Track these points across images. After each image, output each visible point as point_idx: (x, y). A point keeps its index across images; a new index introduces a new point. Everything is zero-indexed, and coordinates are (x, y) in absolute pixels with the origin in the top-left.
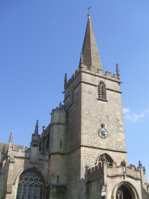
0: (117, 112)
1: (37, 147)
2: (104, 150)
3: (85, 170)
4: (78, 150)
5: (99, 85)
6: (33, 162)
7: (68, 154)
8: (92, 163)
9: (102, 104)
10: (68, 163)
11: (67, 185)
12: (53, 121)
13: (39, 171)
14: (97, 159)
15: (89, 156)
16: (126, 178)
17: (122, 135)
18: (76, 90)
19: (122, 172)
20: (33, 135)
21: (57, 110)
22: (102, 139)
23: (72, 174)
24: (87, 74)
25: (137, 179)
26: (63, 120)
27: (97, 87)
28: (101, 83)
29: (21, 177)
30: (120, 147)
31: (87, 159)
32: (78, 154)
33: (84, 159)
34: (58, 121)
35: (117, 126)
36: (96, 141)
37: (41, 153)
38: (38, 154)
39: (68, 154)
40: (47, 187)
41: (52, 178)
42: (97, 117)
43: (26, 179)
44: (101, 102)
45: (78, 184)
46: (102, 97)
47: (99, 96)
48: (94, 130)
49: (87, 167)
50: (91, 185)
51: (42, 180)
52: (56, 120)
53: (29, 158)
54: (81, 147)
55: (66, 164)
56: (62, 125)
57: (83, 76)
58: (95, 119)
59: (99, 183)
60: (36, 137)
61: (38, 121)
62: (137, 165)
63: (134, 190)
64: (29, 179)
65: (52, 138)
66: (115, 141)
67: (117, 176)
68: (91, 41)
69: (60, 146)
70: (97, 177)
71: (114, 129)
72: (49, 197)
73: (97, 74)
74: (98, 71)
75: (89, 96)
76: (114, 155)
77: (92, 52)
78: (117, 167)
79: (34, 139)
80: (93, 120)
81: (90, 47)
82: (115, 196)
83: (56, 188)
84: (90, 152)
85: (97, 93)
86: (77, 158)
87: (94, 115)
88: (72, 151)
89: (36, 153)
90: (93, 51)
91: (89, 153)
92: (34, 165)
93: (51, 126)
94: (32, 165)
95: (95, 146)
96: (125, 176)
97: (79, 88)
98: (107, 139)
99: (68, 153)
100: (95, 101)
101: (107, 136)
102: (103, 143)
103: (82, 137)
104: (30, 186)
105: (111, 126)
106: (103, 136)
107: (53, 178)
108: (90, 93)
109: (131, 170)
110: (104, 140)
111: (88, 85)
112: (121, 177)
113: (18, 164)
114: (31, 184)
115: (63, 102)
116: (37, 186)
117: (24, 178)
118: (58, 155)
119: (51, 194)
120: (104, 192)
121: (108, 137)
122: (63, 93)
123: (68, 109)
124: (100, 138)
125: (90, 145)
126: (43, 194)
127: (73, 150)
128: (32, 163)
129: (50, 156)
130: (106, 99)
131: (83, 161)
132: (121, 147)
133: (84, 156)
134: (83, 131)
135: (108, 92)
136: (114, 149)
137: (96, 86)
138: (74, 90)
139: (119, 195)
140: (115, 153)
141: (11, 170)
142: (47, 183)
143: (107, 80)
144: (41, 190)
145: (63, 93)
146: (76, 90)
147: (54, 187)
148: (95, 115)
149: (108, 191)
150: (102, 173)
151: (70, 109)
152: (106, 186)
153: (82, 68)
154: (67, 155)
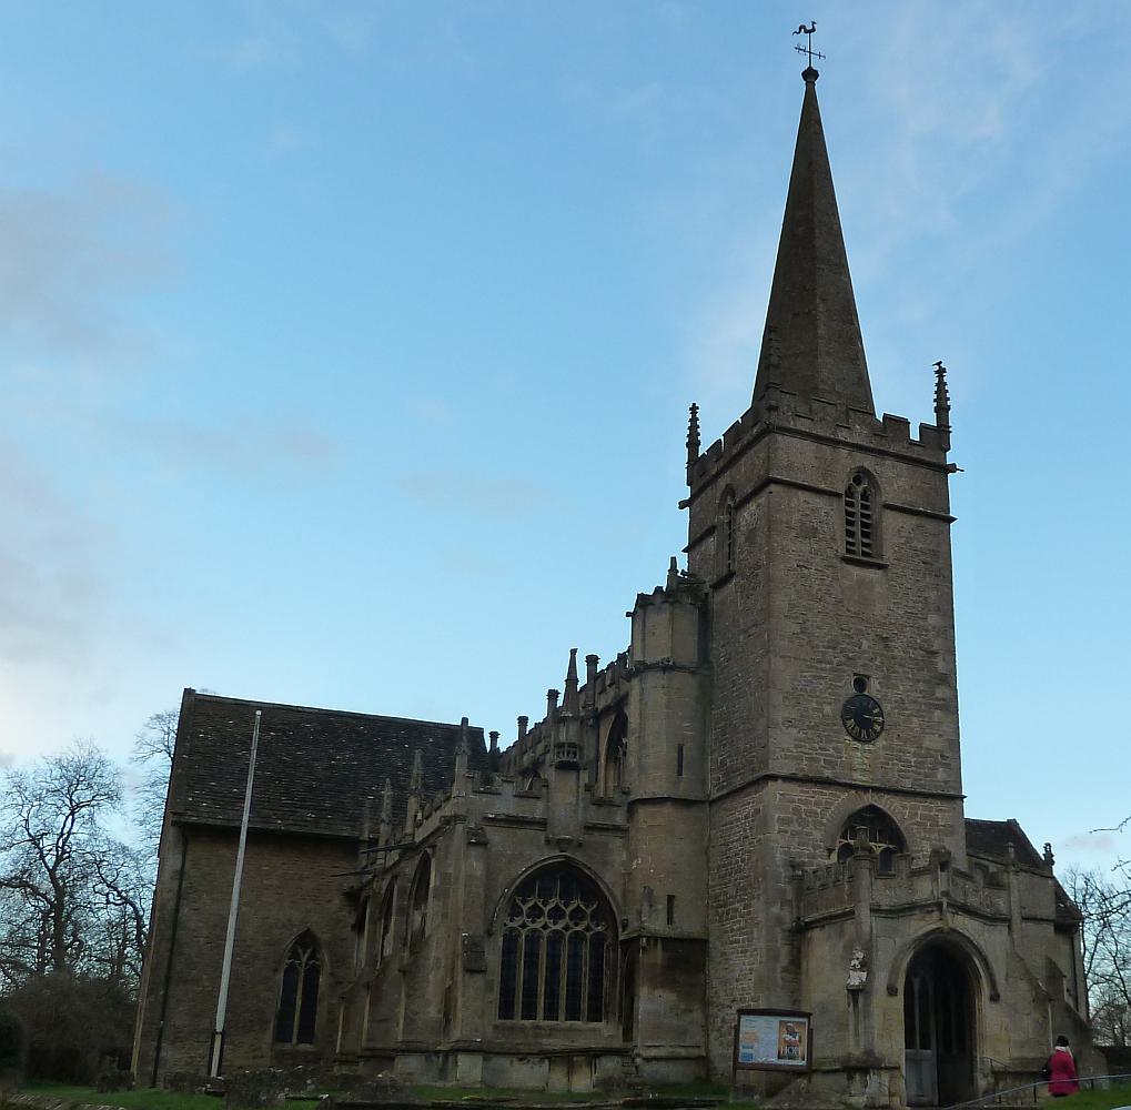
1: (572, 777)
2: (866, 789)
3: (784, 872)
4: (756, 792)
6: (565, 839)
7: (714, 801)
9: (861, 582)
10: (710, 839)
11: (708, 935)
19: (932, 892)
21: (659, 600)
22: (859, 745)
23: (731, 891)
24: (795, 442)
25: (994, 919)
26: (689, 653)
28: (861, 475)
30: (934, 775)
31: (793, 834)
32: (757, 811)
35: (924, 682)
38: (581, 805)
43: (535, 913)
44: (855, 571)
45: (755, 936)
46: (864, 545)
47: (848, 543)
49: (793, 866)
50: (810, 939)
51: (605, 912)
58: (828, 657)
59: (841, 933)
63: (977, 962)
68: (818, 242)
70: (833, 911)
73: (842, 435)
74: (848, 417)
77: (821, 308)
80: (820, 662)
84: (806, 803)
91: (803, 807)
95: (828, 773)
96: (945, 906)
97: (758, 506)
98: (881, 742)
101: (878, 728)
102: (861, 761)
106: (864, 732)
107: (651, 906)
108: (809, 533)
110: (867, 747)
112: (929, 912)
117: (525, 908)
118: (668, 809)
121: (883, 734)
122: (682, 505)
123: (707, 594)
125: (805, 768)
126: (606, 972)
129: (632, 807)
135: (893, 527)
136: (908, 785)
139: (917, 982)
140: (910, 803)
142: (625, 927)
145: (682, 505)
146: (747, 516)
147: (656, 944)
149: (875, 969)
151: (718, 597)
154: (707, 805)
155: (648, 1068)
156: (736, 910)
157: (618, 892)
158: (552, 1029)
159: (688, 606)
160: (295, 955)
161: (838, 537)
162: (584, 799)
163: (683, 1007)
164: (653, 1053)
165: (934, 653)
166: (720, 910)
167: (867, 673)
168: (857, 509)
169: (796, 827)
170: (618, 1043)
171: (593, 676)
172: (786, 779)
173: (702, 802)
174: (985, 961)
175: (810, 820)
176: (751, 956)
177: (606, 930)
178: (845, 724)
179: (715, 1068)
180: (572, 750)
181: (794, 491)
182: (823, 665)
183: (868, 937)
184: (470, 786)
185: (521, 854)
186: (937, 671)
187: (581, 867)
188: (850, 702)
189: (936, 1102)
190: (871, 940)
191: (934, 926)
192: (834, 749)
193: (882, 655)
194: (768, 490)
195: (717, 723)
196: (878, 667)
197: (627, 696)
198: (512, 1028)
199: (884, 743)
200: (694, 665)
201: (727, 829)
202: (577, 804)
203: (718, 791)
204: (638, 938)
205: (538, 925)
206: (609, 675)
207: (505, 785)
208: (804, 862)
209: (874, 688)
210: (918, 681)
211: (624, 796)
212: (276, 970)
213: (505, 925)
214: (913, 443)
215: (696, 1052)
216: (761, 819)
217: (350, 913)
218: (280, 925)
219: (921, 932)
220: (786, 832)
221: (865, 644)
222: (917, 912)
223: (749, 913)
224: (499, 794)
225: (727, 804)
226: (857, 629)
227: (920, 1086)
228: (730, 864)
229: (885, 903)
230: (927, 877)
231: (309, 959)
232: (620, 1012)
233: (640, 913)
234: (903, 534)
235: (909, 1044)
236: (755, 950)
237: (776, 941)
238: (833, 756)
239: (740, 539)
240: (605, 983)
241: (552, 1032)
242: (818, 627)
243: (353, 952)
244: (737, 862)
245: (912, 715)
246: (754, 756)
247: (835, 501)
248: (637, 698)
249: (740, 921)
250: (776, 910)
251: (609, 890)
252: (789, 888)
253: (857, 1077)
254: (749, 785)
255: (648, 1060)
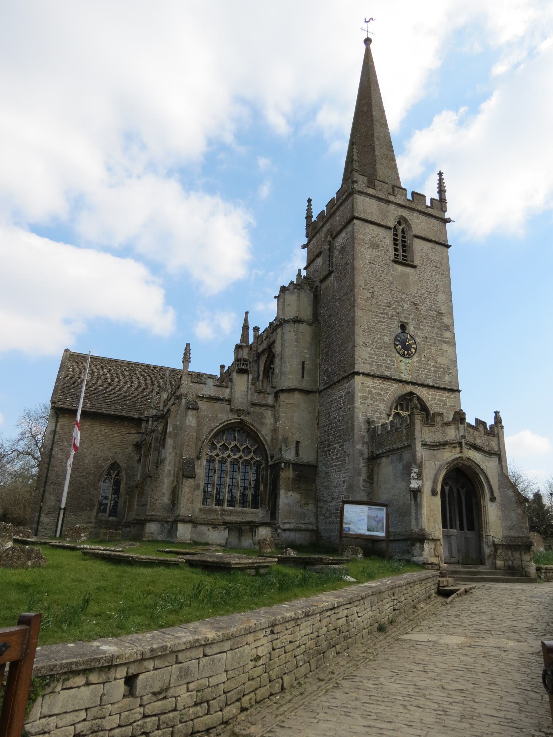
0: (439, 294)
1: (245, 376)
2: (408, 383)
3: (364, 426)
4: (347, 383)
5: (395, 227)
6: (240, 410)
8: (381, 413)
9: (403, 274)
10: (319, 413)
11: (318, 463)
12: (284, 314)
13: (253, 431)
14: (392, 405)
15: (373, 398)
16: (465, 450)
17: (451, 349)
18: (339, 240)
19: (456, 436)
20: (238, 348)
21: (291, 288)
22: (404, 359)
23: (332, 438)
24: (367, 199)
26: (307, 313)
27: (392, 231)
28: (401, 220)
29: (213, 443)
30: (444, 378)
31: (369, 405)
32: (348, 393)
33: (361, 403)
34: (295, 315)
36: (389, 362)
37: (256, 387)
39: (320, 392)
40: (270, 466)
41: (284, 447)
42: (391, 304)
43: (224, 447)
44: (400, 268)
48: (385, 337)
49: (368, 422)
50: (379, 464)
51: (261, 449)
52: (290, 314)
53: (231, 399)
54: (356, 377)
55: (316, 414)
56: (304, 325)
57: (359, 204)
58: (386, 311)
59: (401, 459)
60: (245, 354)
61: (247, 313)
62: (490, 421)
64: (230, 447)
65: (282, 353)
66: (432, 364)
67: (444, 444)
68: (374, 113)
69: (301, 373)
71: (431, 335)
72: (280, 489)
74: (394, 190)
75: (374, 253)
76: (430, 397)
77: (377, 142)
78: (445, 424)
79: (240, 356)
80: (382, 313)
81: (372, 128)
82: (439, 489)
83: (293, 469)
84: (376, 388)
85: (391, 247)
86: (344, 402)
87: (384, 300)
88: (332, 385)
89: (244, 388)
90: (378, 139)
91: (374, 391)
92: (242, 417)
93: (274, 327)
94: (236, 416)
95: (387, 373)
96: (463, 444)
97: (347, 233)
98: (415, 358)
99: (318, 389)
100: (386, 267)
101: (413, 351)
103: (356, 353)
104: (235, 462)
105: (424, 328)
106: (406, 352)
108: (375, 246)
109: (476, 433)
110: (408, 360)
111: (371, 226)
113: (205, 413)
114: (235, 459)
115: (305, 269)
116: (250, 463)
117: (218, 446)
118: (297, 395)
119: (282, 483)
120: (416, 481)
121: (416, 354)
122: (304, 247)
123: (317, 286)
124: (398, 355)
125: (374, 370)
126: (262, 482)
127: (332, 383)
128: (237, 411)
129: (277, 395)
130: (413, 262)
131: (360, 409)
132: (447, 378)
133: (362, 397)
134: (360, 338)
135: (419, 246)
136: (430, 382)
137: (389, 228)
138: (334, 238)
139: (447, 488)
140: (432, 392)
141: (192, 427)
142: (272, 458)
143: (416, 214)
144: (257, 473)
145: (304, 247)
146: (340, 241)
147: (289, 467)
148: (386, 301)
149: (424, 479)
150: (411, 436)
151: (324, 286)
152: (420, 467)
153: (356, 182)
154: (317, 394)
155: (285, 535)
156: (335, 448)
157: (268, 438)
158: (232, 511)
159: (308, 291)
160: (109, 474)
161: (390, 250)
162: (251, 389)
163: (303, 502)
164: (287, 526)
165: (441, 314)
166: (325, 449)
167: (406, 321)
168: (400, 237)
169: (369, 401)
170: (268, 520)
171: (256, 337)
172: (365, 374)
173: (315, 392)
174: (486, 477)
175: (378, 398)
176: (344, 473)
177: (261, 460)
178: (396, 348)
179: (322, 537)
180: (245, 362)
181: (367, 224)
182: (383, 316)
183: (420, 460)
184: (189, 379)
185: (217, 417)
186: (443, 323)
187: (249, 425)
188: (398, 335)
189: (461, 561)
190: (422, 462)
191: (458, 456)
192: (390, 360)
193: (415, 313)
194: (352, 223)
195: (323, 350)
196: (412, 319)
197: (274, 341)
198: (210, 511)
199: (417, 359)
200: (310, 321)
201: (329, 405)
202: (247, 392)
203: (323, 386)
204: (280, 463)
205: (225, 455)
206: (265, 335)
207: (209, 380)
208: (374, 421)
209: (411, 329)
210: (434, 328)
211: (272, 389)
212: (99, 481)
213: (207, 454)
214: (428, 207)
215: (311, 527)
216: (350, 397)
217: (136, 454)
218: (102, 459)
219: (450, 459)
220: (364, 404)
221: (406, 307)
222: (447, 447)
223: (343, 449)
224: (206, 384)
225: (329, 391)
226: (401, 298)
227: (450, 551)
228: (330, 424)
229: (429, 441)
230: (453, 427)
231: (116, 476)
232: (269, 504)
233: (280, 450)
234: (424, 251)
235: (444, 526)
236: (347, 470)
237: (359, 465)
238: (389, 364)
239: (336, 253)
240: (261, 488)
241: (231, 513)
242: (381, 295)
243: (137, 474)
244: (335, 422)
245: (430, 345)
246: (345, 364)
247: (388, 231)
248: (280, 338)
249: (337, 454)
250: (359, 447)
251: (264, 438)
252: (366, 435)
253: (418, 545)
254: (344, 378)
255: (284, 530)
